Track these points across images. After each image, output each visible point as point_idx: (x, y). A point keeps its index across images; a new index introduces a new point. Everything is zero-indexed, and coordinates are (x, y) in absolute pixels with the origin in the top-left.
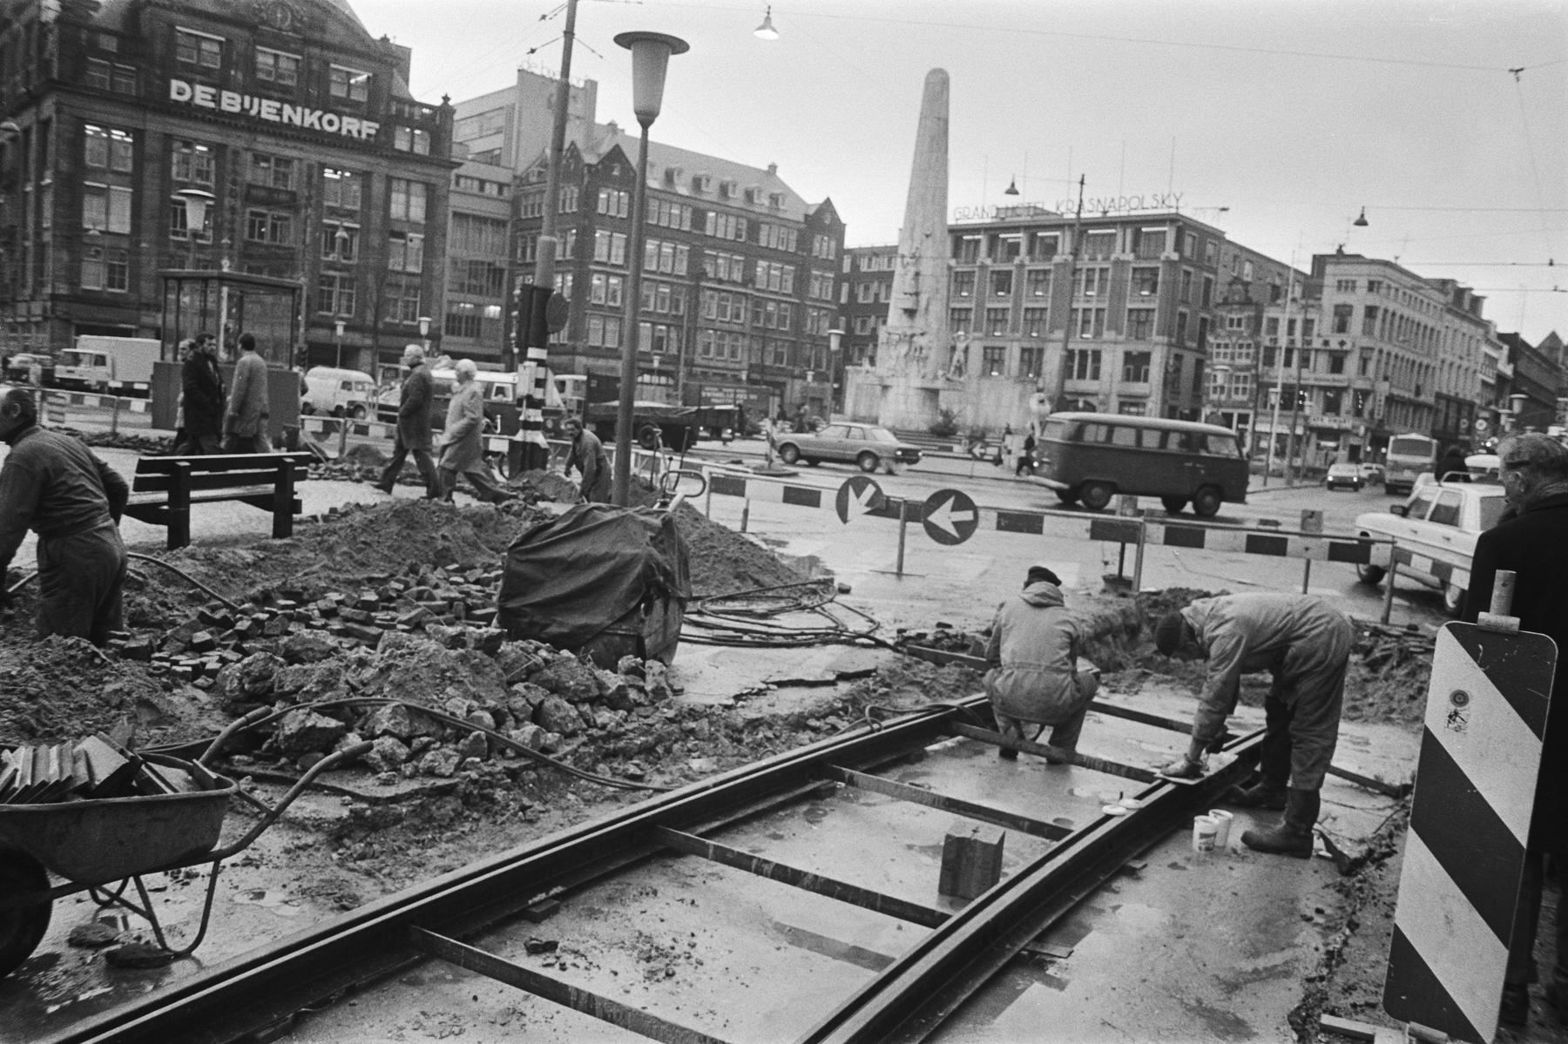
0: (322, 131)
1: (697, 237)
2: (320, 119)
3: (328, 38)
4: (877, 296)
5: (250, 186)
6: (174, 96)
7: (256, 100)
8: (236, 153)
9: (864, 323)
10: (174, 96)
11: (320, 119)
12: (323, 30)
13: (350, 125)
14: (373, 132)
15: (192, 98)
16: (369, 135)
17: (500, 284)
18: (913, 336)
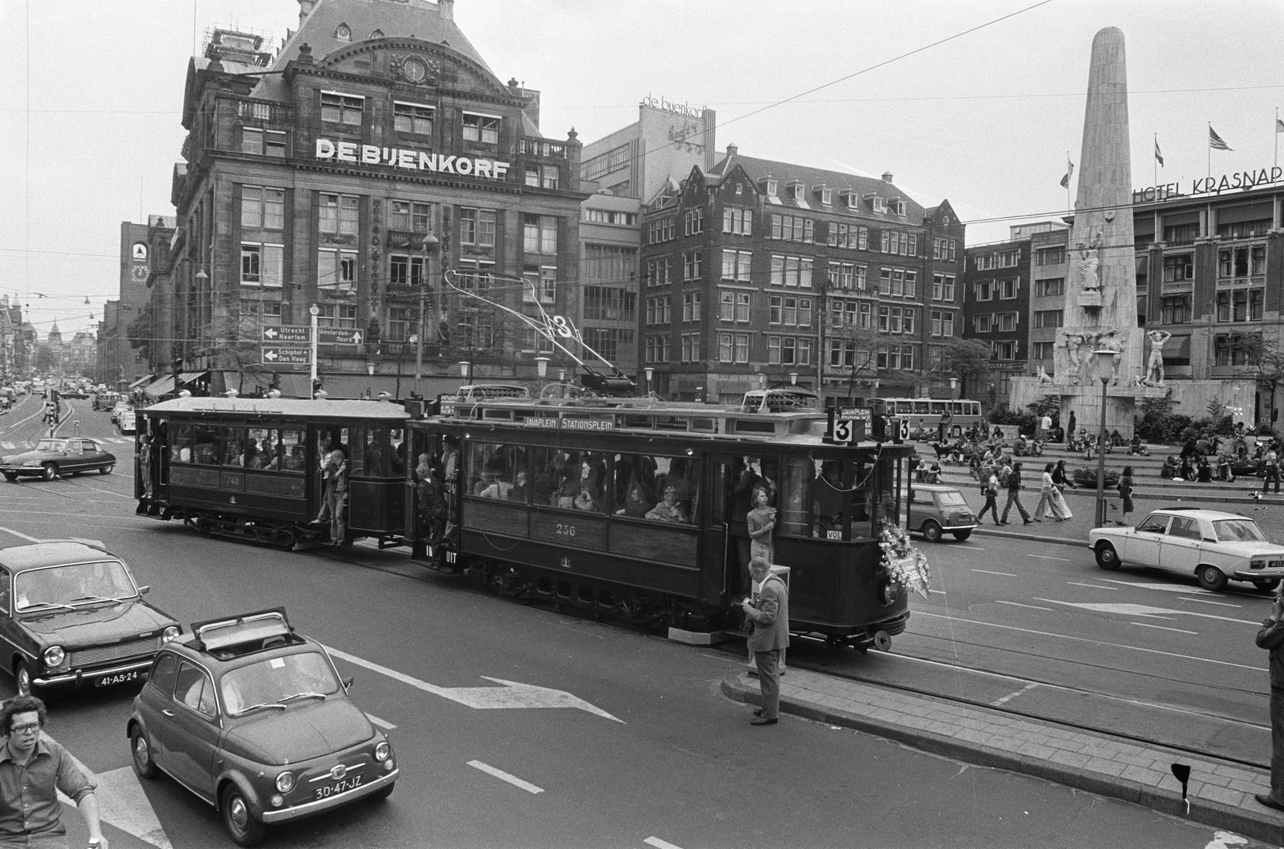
0: (457, 175)
1: (821, 249)
2: (454, 163)
3: (459, 87)
4: (996, 293)
5: (390, 232)
6: (319, 154)
7: (394, 151)
8: (377, 202)
9: (984, 321)
10: (319, 154)
11: (454, 163)
12: (454, 80)
13: (483, 166)
14: (504, 171)
15: (335, 155)
16: (500, 174)
17: (632, 308)
18: (1099, 337)
